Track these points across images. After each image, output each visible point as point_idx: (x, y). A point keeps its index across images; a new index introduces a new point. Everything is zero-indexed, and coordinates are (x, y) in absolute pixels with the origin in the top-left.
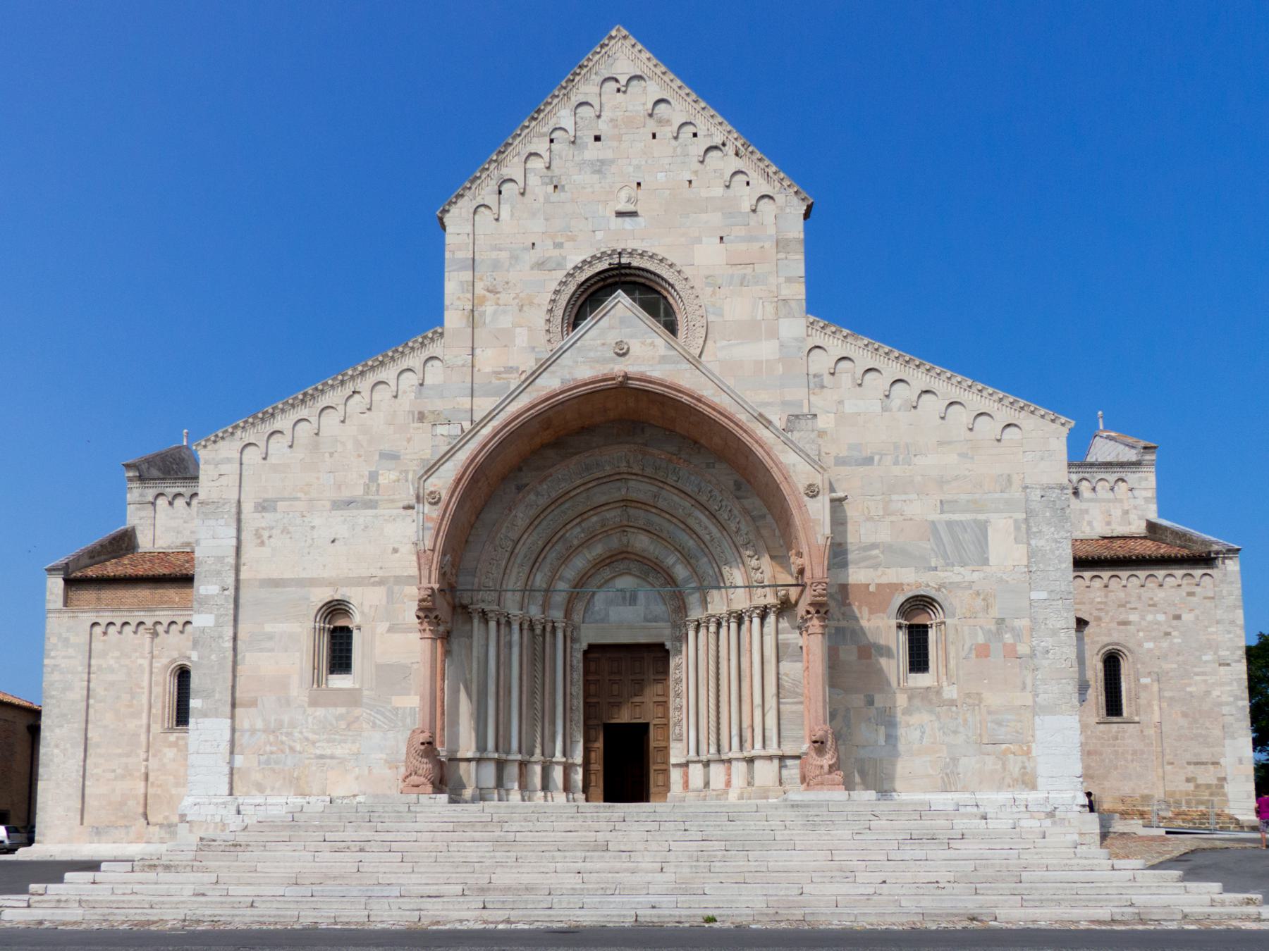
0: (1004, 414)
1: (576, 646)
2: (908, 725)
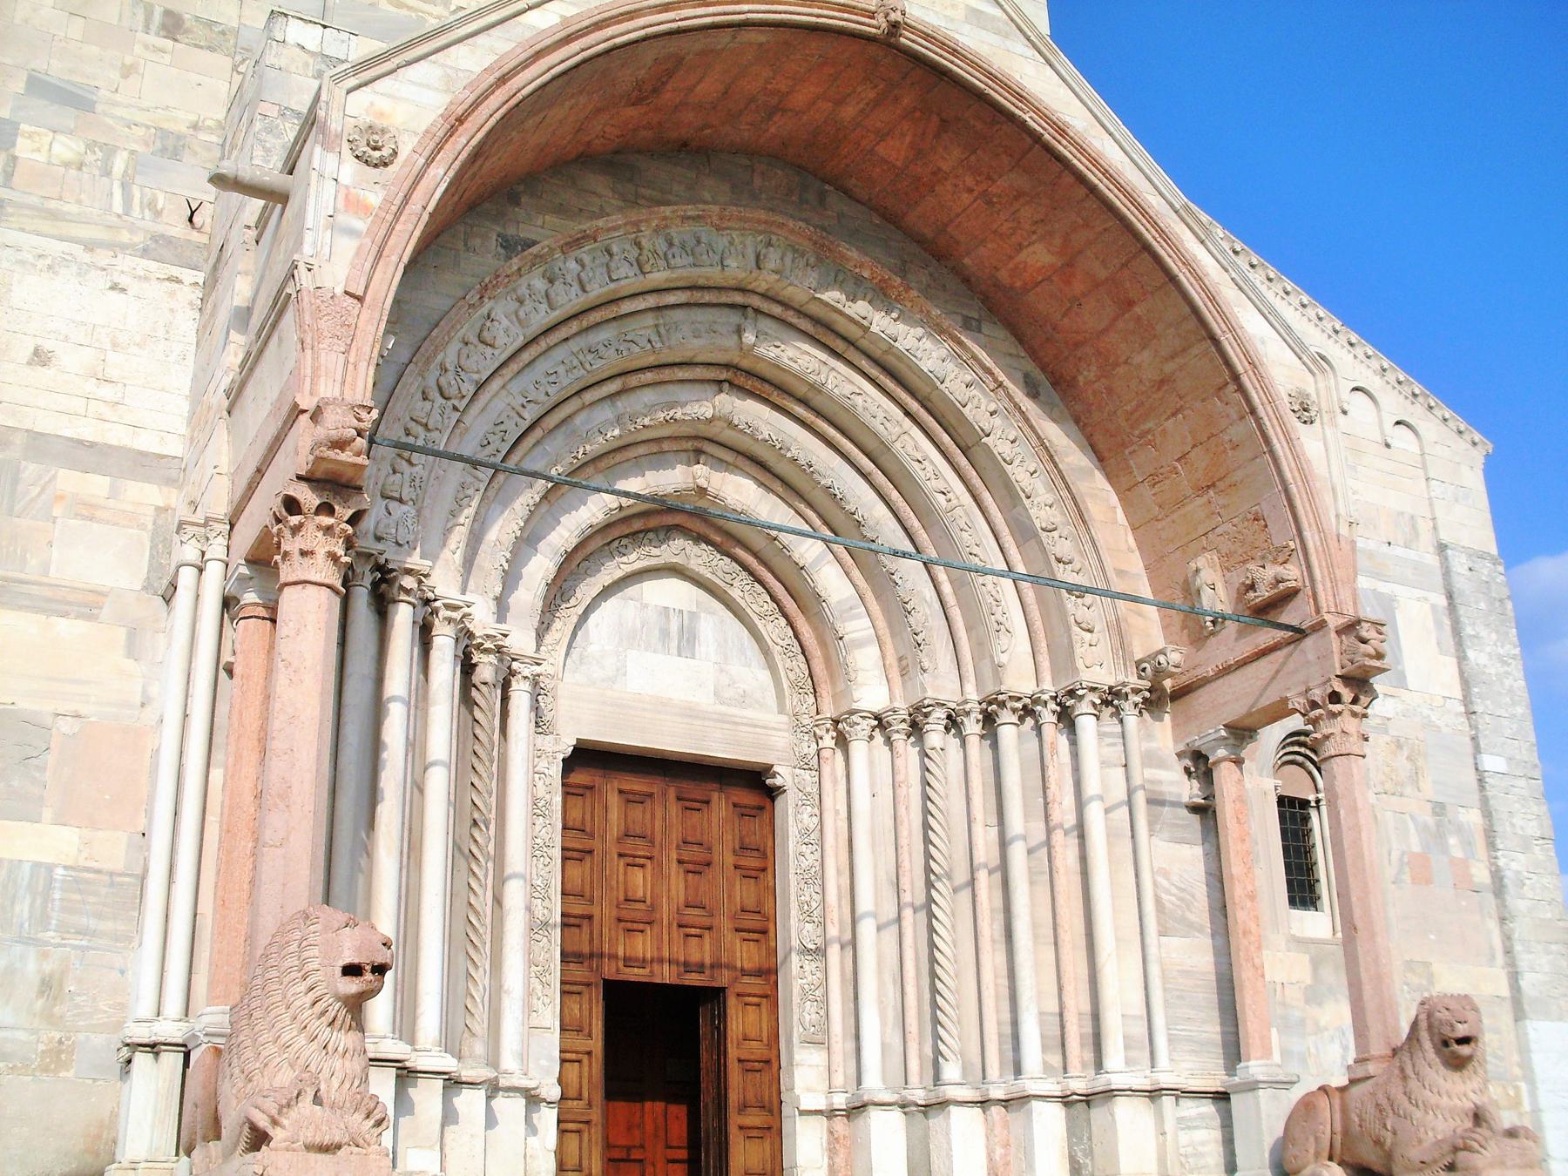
0: (1394, 403)
1: (546, 743)
2: (1319, 1030)
